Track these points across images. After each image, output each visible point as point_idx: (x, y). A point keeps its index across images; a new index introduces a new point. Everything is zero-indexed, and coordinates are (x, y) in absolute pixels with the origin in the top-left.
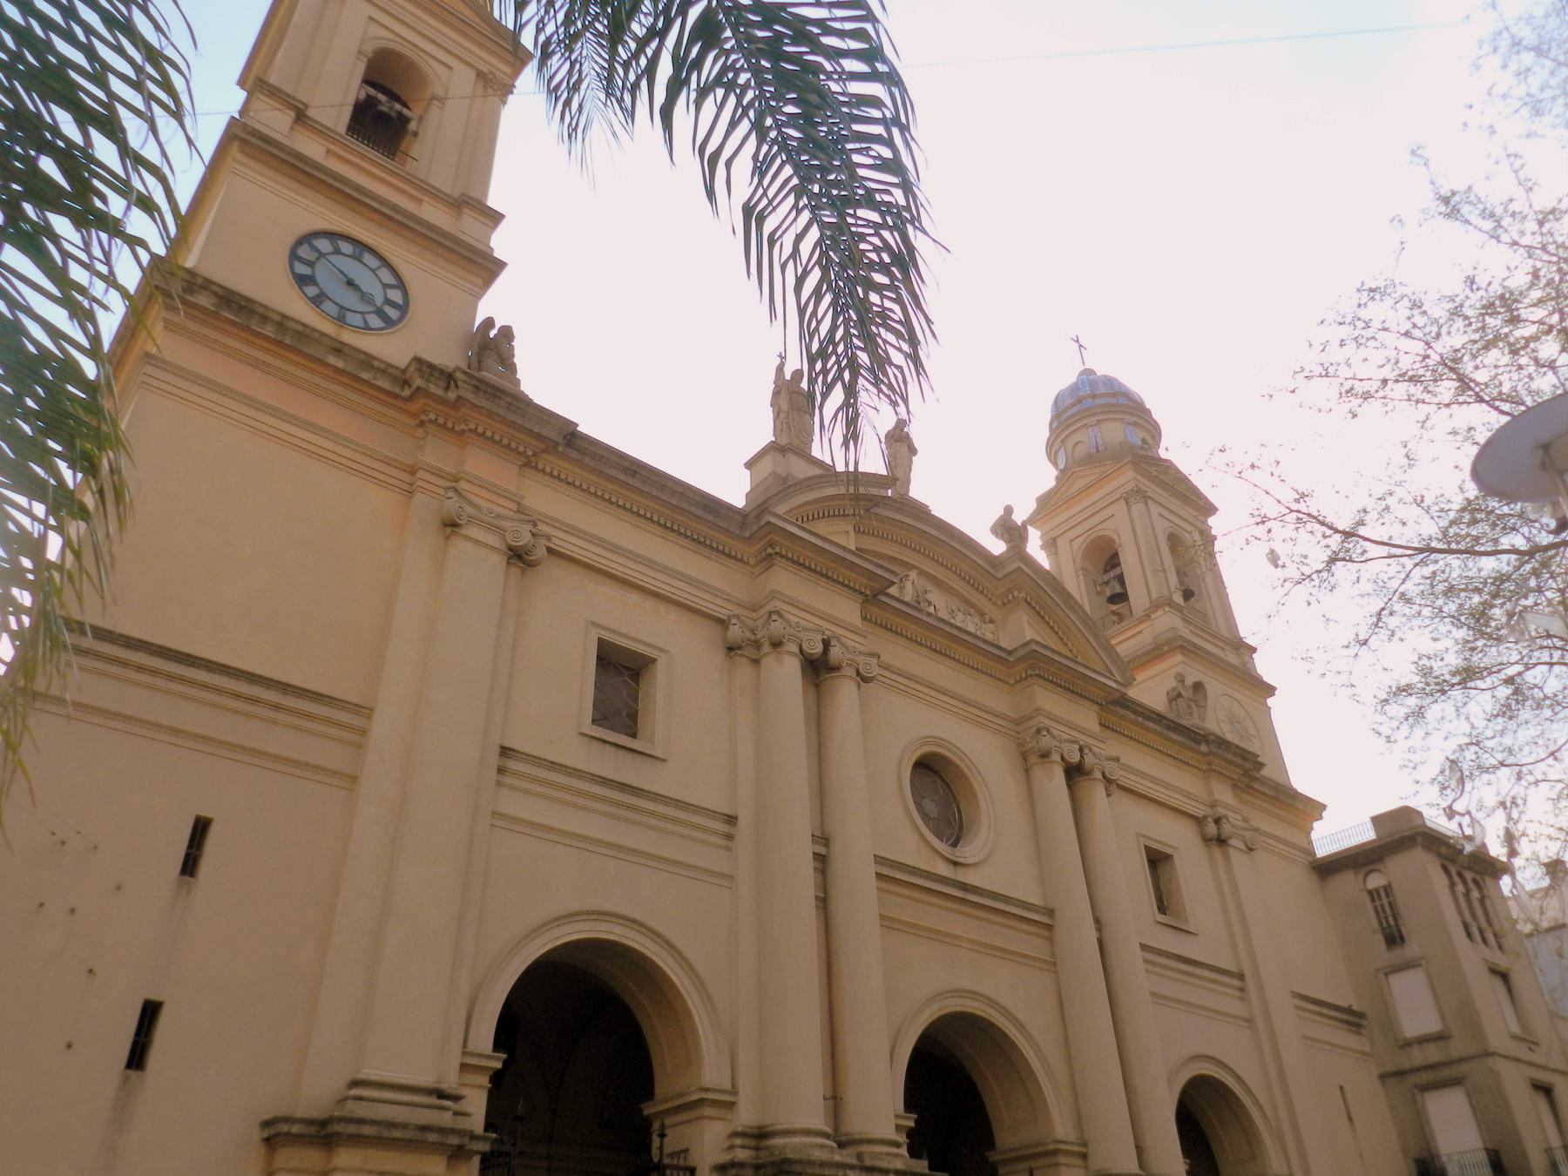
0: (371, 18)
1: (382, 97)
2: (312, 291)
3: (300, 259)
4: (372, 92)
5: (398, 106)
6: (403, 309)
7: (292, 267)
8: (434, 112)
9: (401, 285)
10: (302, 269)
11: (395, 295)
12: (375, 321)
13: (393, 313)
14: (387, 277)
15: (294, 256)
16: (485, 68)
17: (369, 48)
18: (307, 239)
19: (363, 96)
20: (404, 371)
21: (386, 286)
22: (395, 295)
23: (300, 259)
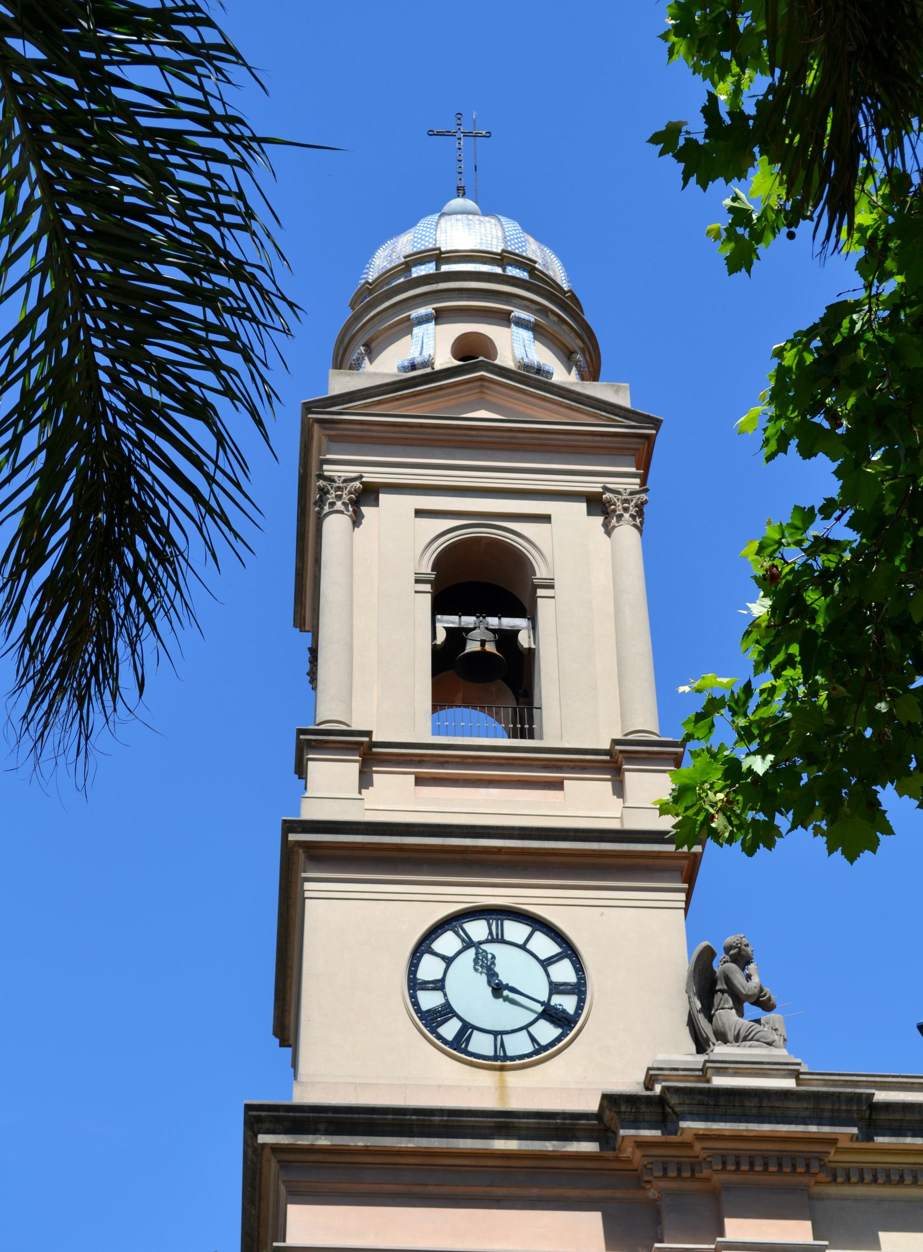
0: (419, 513)
1: (468, 621)
2: (450, 1029)
3: (425, 986)
4: (452, 621)
5: (493, 622)
6: (579, 989)
7: (415, 1003)
8: (544, 608)
9: (569, 950)
10: (429, 1000)
11: (564, 972)
12: (546, 1032)
13: (568, 1003)
14: (544, 946)
15: (414, 985)
16: (593, 485)
17: (426, 567)
18: (423, 946)
19: (441, 637)
20: (598, 1116)
21: (546, 964)
22: (564, 972)
23: (425, 986)
